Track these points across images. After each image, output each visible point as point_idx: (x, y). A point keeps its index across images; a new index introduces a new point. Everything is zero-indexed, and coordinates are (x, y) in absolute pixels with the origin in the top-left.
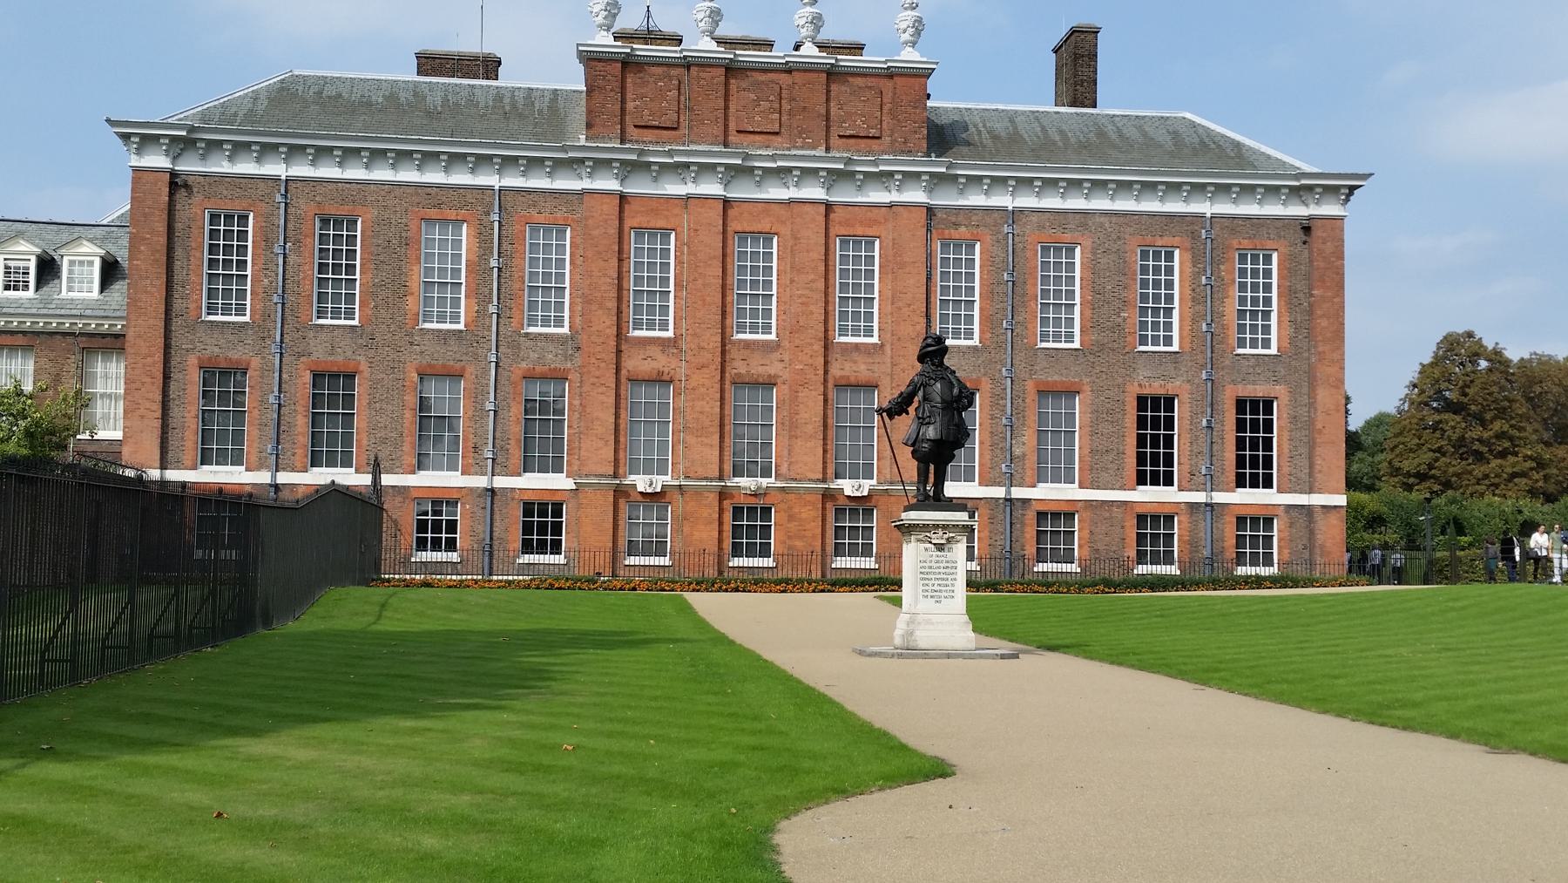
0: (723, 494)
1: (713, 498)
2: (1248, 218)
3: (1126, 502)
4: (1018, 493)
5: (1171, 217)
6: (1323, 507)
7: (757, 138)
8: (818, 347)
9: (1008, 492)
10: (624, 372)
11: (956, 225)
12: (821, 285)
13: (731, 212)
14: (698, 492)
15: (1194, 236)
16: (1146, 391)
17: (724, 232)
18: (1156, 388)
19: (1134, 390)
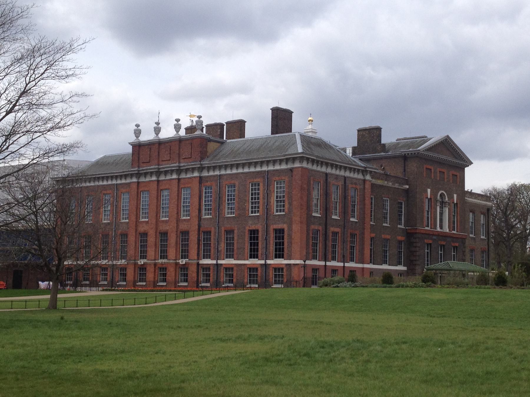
0: (155, 265)
1: (153, 266)
2: (277, 170)
3: (245, 264)
4: (220, 262)
5: (258, 172)
6: (294, 264)
7: (166, 162)
8: (175, 221)
9: (217, 262)
10: (138, 232)
11: (207, 181)
12: (176, 203)
13: (160, 184)
14: (150, 264)
15: (264, 177)
16: (251, 229)
17: (158, 190)
18: (253, 227)
19: (247, 228)
